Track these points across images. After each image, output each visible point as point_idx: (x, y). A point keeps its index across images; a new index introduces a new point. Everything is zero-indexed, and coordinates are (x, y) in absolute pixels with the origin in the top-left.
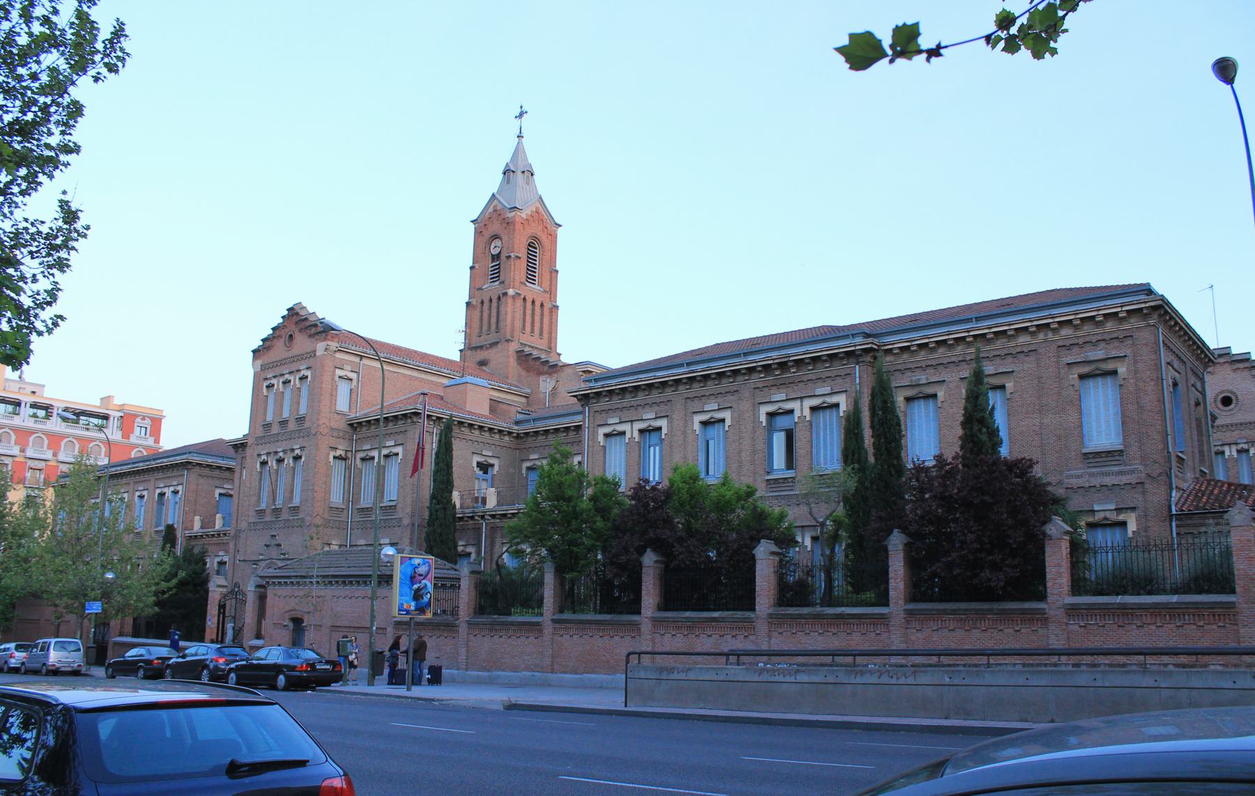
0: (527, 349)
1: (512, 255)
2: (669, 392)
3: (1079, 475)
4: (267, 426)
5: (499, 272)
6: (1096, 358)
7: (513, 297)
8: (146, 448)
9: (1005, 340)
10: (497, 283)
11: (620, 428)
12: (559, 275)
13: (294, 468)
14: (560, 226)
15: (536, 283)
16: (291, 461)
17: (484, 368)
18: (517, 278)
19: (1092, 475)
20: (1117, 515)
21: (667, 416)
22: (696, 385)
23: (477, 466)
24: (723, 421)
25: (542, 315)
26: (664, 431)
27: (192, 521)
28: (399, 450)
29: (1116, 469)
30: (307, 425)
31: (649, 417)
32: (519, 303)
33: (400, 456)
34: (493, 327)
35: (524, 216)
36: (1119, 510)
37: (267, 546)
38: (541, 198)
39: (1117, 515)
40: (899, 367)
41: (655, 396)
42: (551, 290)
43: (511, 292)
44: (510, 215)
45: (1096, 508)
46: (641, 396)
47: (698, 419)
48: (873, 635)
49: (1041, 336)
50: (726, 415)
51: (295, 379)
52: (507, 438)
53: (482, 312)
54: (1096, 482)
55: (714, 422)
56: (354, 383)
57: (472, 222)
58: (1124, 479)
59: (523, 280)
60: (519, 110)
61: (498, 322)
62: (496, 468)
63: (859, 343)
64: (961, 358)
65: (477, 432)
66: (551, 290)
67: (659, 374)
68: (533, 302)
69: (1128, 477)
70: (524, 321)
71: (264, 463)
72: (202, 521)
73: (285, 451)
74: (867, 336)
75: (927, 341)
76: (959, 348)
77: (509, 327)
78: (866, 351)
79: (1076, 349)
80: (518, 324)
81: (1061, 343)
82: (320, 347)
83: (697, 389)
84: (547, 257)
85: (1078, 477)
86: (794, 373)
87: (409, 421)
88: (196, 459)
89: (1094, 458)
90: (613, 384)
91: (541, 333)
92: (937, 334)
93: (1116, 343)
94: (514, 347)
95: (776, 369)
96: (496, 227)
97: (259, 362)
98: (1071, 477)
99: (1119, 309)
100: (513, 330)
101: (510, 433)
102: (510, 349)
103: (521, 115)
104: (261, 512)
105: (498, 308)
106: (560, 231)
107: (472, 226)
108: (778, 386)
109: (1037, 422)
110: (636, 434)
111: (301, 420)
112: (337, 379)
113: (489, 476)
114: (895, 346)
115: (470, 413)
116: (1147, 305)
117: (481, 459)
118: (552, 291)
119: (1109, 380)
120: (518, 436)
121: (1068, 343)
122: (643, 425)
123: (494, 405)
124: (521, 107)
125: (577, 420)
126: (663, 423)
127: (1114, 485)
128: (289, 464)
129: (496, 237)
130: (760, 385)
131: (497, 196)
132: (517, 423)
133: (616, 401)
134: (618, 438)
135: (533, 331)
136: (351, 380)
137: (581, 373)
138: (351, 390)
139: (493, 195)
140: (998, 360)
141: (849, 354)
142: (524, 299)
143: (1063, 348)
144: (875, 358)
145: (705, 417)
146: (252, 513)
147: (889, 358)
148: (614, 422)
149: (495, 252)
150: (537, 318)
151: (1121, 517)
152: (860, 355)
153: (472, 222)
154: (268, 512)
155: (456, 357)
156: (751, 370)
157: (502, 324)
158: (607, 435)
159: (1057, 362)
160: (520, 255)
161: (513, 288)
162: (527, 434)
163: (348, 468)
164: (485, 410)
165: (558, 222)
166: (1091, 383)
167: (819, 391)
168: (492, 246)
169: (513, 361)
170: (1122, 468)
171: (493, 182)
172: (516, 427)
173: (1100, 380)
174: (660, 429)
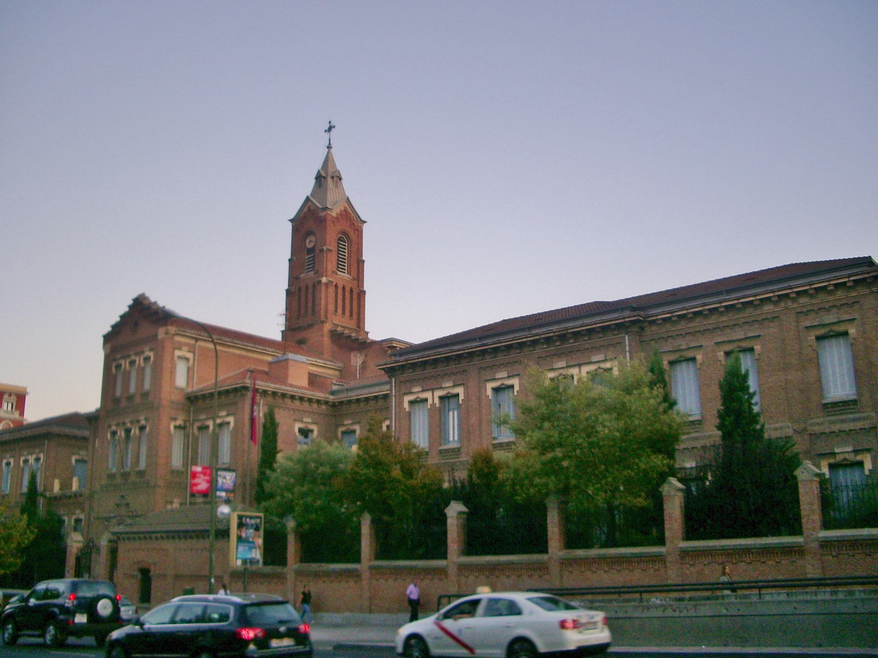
0: (339, 329)
1: (325, 248)
2: (464, 364)
3: (820, 423)
4: (117, 401)
5: (314, 263)
7: (327, 285)
8: (13, 421)
9: (751, 309)
10: (313, 272)
12: (365, 264)
13: (140, 438)
14: (365, 222)
15: (346, 271)
16: (137, 431)
17: (303, 346)
18: (329, 268)
20: (855, 456)
21: (463, 384)
23: (299, 432)
24: (512, 387)
25: (352, 299)
26: (461, 397)
27: (52, 485)
28: (231, 419)
29: (851, 416)
31: (448, 387)
32: (331, 290)
33: (232, 425)
34: (310, 311)
35: (334, 214)
36: (856, 452)
37: (118, 505)
38: (348, 199)
39: (855, 456)
40: (662, 335)
41: (452, 367)
42: (358, 277)
43: (324, 280)
44: (322, 214)
45: (837, 450)
46: (441, 368)
49: (782, 304)
50: (515, 382)
52: (324, 407)
54: (836, 428)
55: (504, 389)
57: (290, 220)
58: (859, 425)
59: (335, 269)
61: (314, 305)
62: (315, 433)
63: (628, 316)
65: (297, 403)
66: (358, 277)
67: (455, 348)
68: (344, 288)
69: (862, 423)
73: (132, 422)
74: (634, 309)
75: (685, 312)
76: (714, 317)
77: (322, 313)
78: (634, 323)
79: (813, 315)
80: (331, 307)
81: (799, 310)
82: (161, 332)
83: (488, 360)
84: (354, 248)
86: (572, 343)
87: (239, 394)
88: (55, 429)
89: (832, 407)
90: (415, 358)
91: (351, 315)
92: (695, 306)
94: (327, 327)
95: (557, 340)
97: (109, 346)
99: (846, 280)
101: (326, 403)
102: (325, 329)
103: (330, 129)
104: (111, 476)
106: (365, 228)
108: (559, 355)
110: (437, 401)
111: (145, 395)
112: (176, 358)
113: (308, 440)
114: (658, 317)
115: (291, 385)
116: (870, 275)
117: (301, 425)
119: (841, 340)
120: (333, 405)
123: (313, 380)
124: (330, 122)
125: (384, 390)
126: (460, 390)
127: (851, 430)
129: (310, 233)
132: (333, 393)
133: (418, 373)
134: (421, 405)
135: (344, 313)
136: (187, 359)
138: (189, 369)
139: (308, 197)
140: (746, 327)
141: (620, 327)
142: (336, 286)
144: (642, 329)
147: (654, 328)
148: (501, 377)
150: (347, 302)
151: (859, 458)
152: (629, 327)
153: (290, 220)
155: (278, 337)
156: (535, 343)
157: (317, 308)
158: (411, 403)
160: (331, 248)
161: (326, 276)
162: (341, 403)
163: (187, 436)
164: (304, 382)
165: (363, 219)
166: (826, 343)
167: (595, 358)
168: (308, 241)
169: (327, 341)
170: (857, 415)
171: (307, 187)
172: (332, 397)
173: (834, 342)
174: (457, 395)
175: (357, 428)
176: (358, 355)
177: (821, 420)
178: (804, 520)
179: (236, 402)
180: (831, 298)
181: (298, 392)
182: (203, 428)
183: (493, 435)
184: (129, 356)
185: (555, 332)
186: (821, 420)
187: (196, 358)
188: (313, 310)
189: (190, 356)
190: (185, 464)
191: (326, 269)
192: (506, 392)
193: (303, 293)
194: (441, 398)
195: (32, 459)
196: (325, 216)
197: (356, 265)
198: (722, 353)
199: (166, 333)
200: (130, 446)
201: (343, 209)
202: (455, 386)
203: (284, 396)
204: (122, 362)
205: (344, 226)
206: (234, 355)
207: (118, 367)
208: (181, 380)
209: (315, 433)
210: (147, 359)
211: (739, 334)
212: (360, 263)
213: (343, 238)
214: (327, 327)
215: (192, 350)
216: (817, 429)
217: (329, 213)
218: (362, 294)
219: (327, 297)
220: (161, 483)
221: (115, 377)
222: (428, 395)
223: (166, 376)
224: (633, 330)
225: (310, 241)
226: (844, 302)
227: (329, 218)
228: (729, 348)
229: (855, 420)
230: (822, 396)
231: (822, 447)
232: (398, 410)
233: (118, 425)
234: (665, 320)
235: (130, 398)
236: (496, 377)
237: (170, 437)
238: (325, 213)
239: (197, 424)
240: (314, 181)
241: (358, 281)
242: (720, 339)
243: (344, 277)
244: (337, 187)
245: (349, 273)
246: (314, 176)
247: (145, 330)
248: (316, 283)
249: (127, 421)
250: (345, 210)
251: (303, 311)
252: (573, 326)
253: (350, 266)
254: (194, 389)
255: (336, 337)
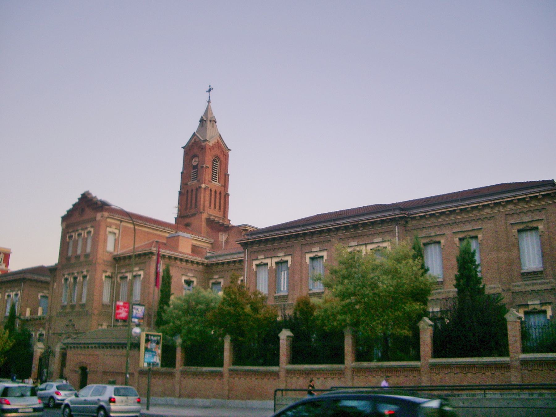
0: (212, 217)
1: (204, 166)
2: (292, 242)
3: (519, 285)
4: (69, 259)
5: (197, 175)
6: (526, 221)
7: (205, 189)
9: (477, 212)
11: (265, 261)
13: (83, 282)
14: (231, 150)
15: (217, 181)
16: (81, 278)
17: (188, 227)
18: (207, 178)
19: (526, 285)
21: (291, 255)
22: (307, 237)
24: (322, 257)
26: (290, 263)
28: (142, 273)
29: (539, 281)
30: (91, 258)
31: (281, 256)
32: (208, 193)
33: (142, 276)
34: (193, 206)
35: (211, 144)
36: (542, 304)
37: (67, 326)
38: (220, 135)
39: (541, 307)
40: (419, 227)
41: (284, 243)
42: (225, 184)
43: (203, 186)
44: (203, 144)
45: (529, 303)
46: (276, 244)
47: (308, 256)
48: (411, 377)
49: (497, 209)
50: (324, 254)
51: (84, 233)
52: (201, 267)
53: (187, 196)
54: (528, 289)
56: (117, 235)
57: (183, 147)
58: (544, 287)
59: (210, 180)
60: (209, 88)
62: (195, 283)
63: (398, 214)
64: (453, 222)
65: (184, 263)
66: (225, 184)
67: (287, 231)
68: (215, 192)
69: (546, 285)
70: (210, 202)
71: (66, 280)
72: (31, 311)
73: (78, 273)
74: (402, 210)
75: (434, 212)
76: (453, 216)
79: (515, 216)
80: (207, 204)
81: (507, 213)
82: (99, 216)
83: (308, 240)
84: (223, 167)
85: (518, 286)
86: (362, 230)
87: (147, 257)
88: (29, 276)
90: (261, 237)
91: (220, 209)
92: (440, 208)
93: (537, 213)
94: (205, 216)
95: (352, 228)
96: (196, 151)
97: (65, 224)
98: (515, 286)
100: (204, 206)
101: (203, 264)
103: (210, 90)
104: (64, 307)
105: (196, 195)
106: (230, 153)
107: (183, 150)
108: (354, 237)
109: (495, 256)
110: (274, 265)
111: (87, 256)
112: (107, 233)
113: (191, 288)
114: (418, 215)
117: (186, 278)
118: (225, 185)
119: (534, 233)
121: (511, 213)
122: (277, 260)
123: (195, 249)
124: (210, 86)
125: (240, 257)
126: (289, 258)
127: (538, 290)
128: (80, 279)
129: (195, 156)
130: (343, 237)
131: (196, 133)
132: (207, 258)
133: (262, 246)
135: (215, 207)
136: (115, 234)
137: (242, 231)
138: (115, 239)
139: (194, 133)
140: (473, 223)
141: (392, 220)
142: (211, 190)
143: (508, 216)
144: (407, 222)
145: (312, 255)
146: (59, 307)
147: (414, 222)
149: (194, 164)
150: (218, 200)
151: (543, 308)
153: (183, 147)
154: (68, 307)
156: (338, 229)
158: (257, 265)
159: (506, 223)
160: (208, 166)
161: (205, 184)
162: (212, 265)
163: (113, 283)
164: (189, 251)
165: (229, 148)
166: (524, 234)
167: (376, 240)
168: (193, 161)
169: (204, 224)
170: (542, 281)
171: (194, 127)
172: (206, 261)
173: (529, 233)
174: (287, 262)
175: (222, 281)
176: (224, 234)
177: (519, 283)
178: (510, 347)
179: (145, 262)
180: (528, 205)
181: (185, 257)
182: (124, 278)
183: (309, 288)
184: (77, 231)
185: (350, 223)
186: (519, 283)
187: (120, 233)
188: (196, 205)
189: (117, 231)
190: (111, 300)
191: (205, 179)
192: (318, 260)
193: (190, 194)
194: (277, 263)
195: (13, 295)
196: (205, 145)
197: (223, 177)
198: (457, 239)
199: (102, 217)
200: (76, 288)
201: (216, 141)
202: (285, 255)
203: (176, 259)
204: (73, 234)
205: (217, 152)
206: (145, 232)
207: (71, 237)
208: (110, 247)
209: (195, 283)
210: (89, 233)
211: (469, 227)
212: (226, 176)
213: (216, 160)
214: (205, 216)
215: (118, 228)
216: (517, 289)
217: (208, 143)
218: (227, 195)
219: (205, 197)
220: (96, 312)
221: (68, 243)
222: (268, 261)
223: (101, 244)
224: (401, 222)
225: (195, 161)
226: (536, 208)
227: (207, 146)
228: (461, 236)
229: (541, 284)
230: (520, 268)
231: (520, 300)
232: (249, 270)
233: (69, 274)
234: (422, 217)
235: (78, 257)
236: (312, 251)
237: (102, 283)
238: (205, 143)
239: (119, 275)
240: (198, 123)
241: (225, 187)
242: (456, 230)
243: (216, 184)
244: (213, 127)
245: (219, 182)
246: (199, 119)
247: (89, 214)
248: (198, 188)
249: (75, 272)
250: (218, 142)
251: (189, 206)
252: (362, 219)
253: (220, 178)
254: (119, 253)
255: (210, 222)
